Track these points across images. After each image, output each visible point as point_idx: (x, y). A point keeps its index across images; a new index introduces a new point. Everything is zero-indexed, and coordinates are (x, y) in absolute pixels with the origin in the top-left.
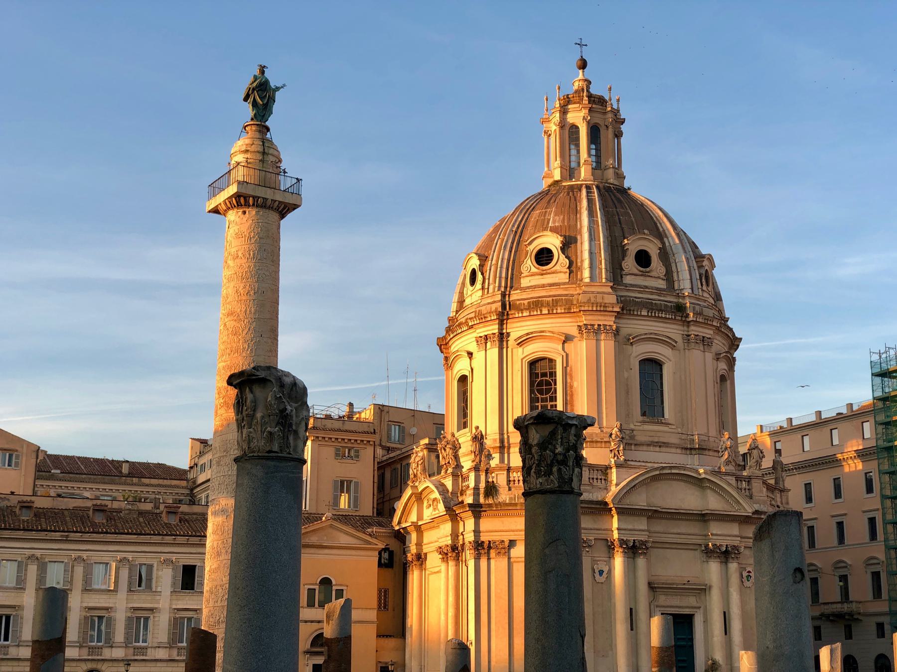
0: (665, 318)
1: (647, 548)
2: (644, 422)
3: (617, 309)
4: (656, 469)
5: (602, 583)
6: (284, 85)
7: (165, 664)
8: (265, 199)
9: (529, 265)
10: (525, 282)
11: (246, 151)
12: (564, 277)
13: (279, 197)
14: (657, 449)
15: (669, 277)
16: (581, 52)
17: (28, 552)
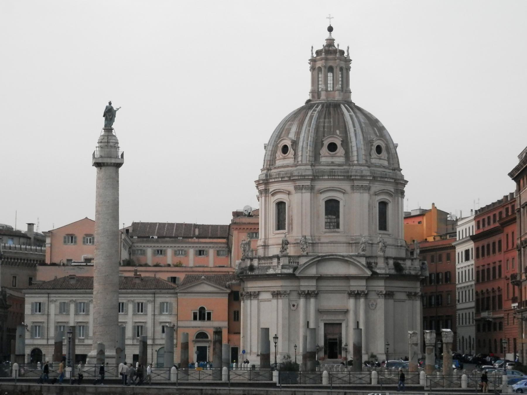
0: (338, 179)
1: (317, 294)
2: (326, 232)
3: (311, 177)
4: (319, 257)
5: (294, 310)
6: (120, 108)
7: (130, 346)
8: (107, 163)
9: (279, 154)
10: (278, 163)
11: (101, 142)
12: (290, 161)
13: (113, 161)
14: (333, 245)
15: (347, 155)
16: (330, 22)
17: (71, 299)
